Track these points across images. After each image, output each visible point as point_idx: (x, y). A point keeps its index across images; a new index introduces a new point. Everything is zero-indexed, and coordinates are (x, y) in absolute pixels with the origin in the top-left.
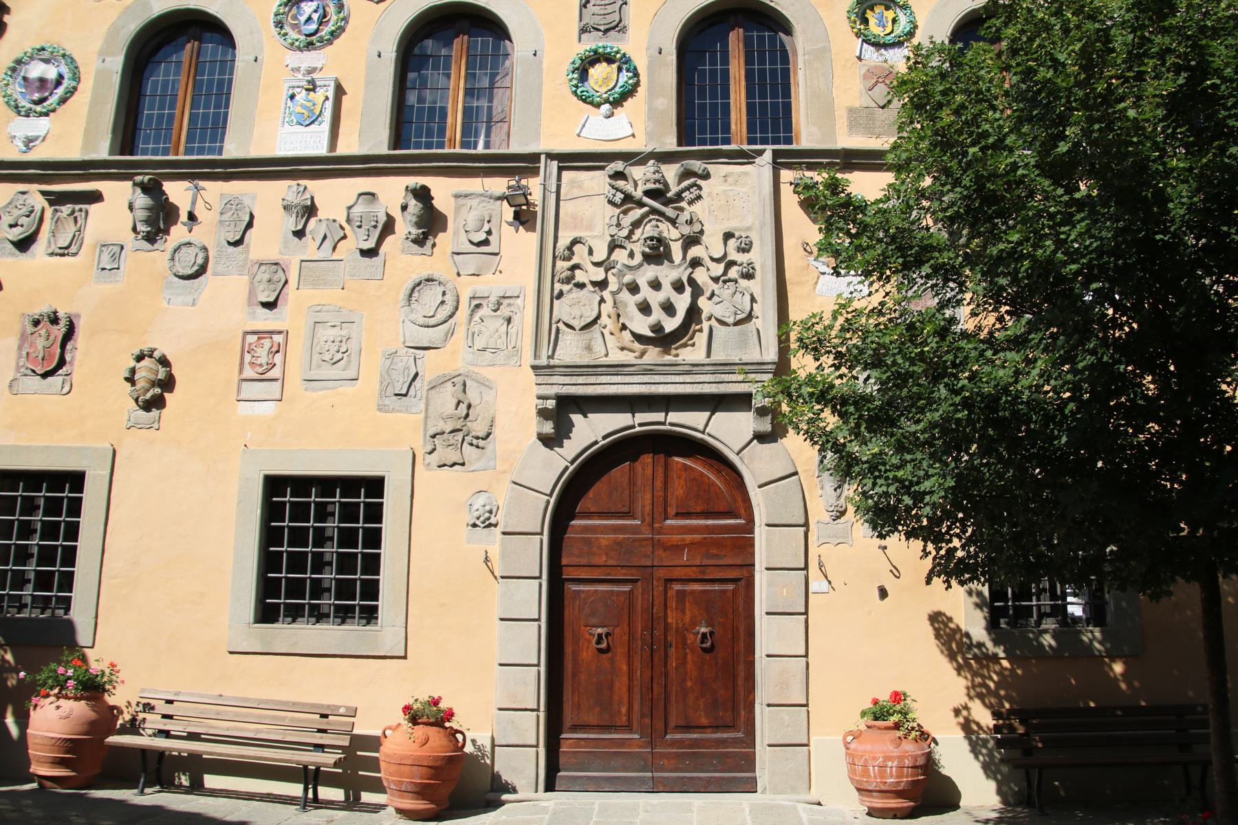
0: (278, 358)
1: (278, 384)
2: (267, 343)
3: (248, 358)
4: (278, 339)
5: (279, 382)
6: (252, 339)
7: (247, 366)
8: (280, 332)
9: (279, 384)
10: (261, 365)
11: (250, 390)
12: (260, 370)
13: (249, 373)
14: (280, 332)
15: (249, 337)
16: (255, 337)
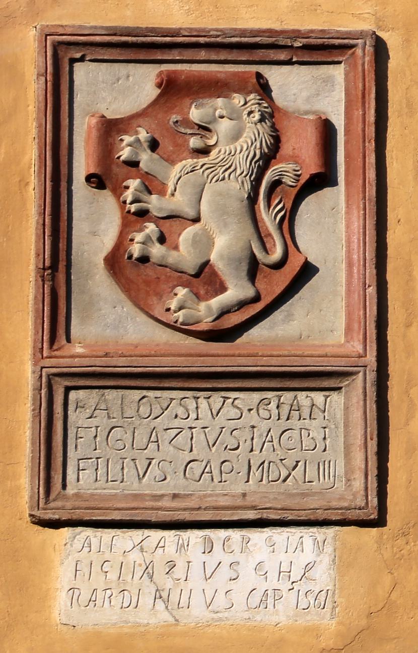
0: (328, 229)
1: (345, 407)
2: (234, 129)
3: (97, 224)
4: (314, 93)
5: (359, 388)
6: (114, 91)
7: (95, 286)
8: (319, 50)
9: (345, 407)
10: (204, 278)
11: (116, 449)
12: (206, 311)
13: (109, 322)
14: (319, 50)
15: (85, 74)
16: (139, 85)
